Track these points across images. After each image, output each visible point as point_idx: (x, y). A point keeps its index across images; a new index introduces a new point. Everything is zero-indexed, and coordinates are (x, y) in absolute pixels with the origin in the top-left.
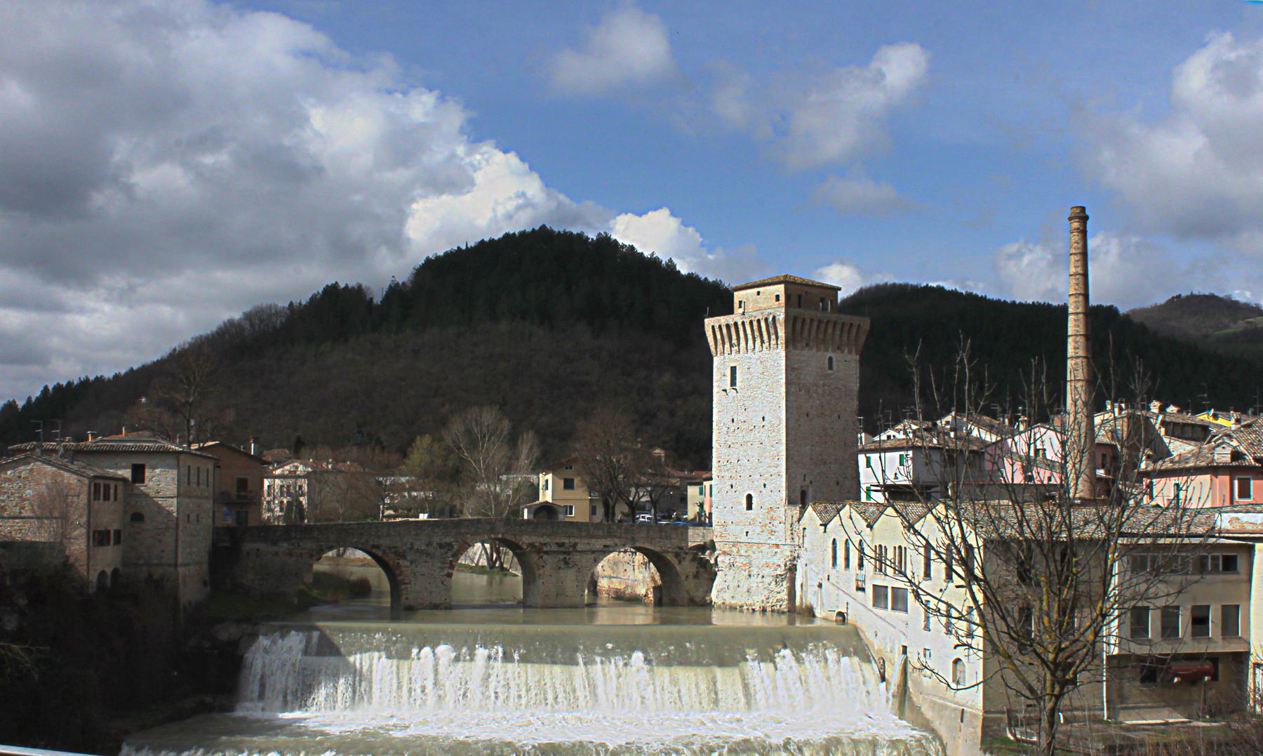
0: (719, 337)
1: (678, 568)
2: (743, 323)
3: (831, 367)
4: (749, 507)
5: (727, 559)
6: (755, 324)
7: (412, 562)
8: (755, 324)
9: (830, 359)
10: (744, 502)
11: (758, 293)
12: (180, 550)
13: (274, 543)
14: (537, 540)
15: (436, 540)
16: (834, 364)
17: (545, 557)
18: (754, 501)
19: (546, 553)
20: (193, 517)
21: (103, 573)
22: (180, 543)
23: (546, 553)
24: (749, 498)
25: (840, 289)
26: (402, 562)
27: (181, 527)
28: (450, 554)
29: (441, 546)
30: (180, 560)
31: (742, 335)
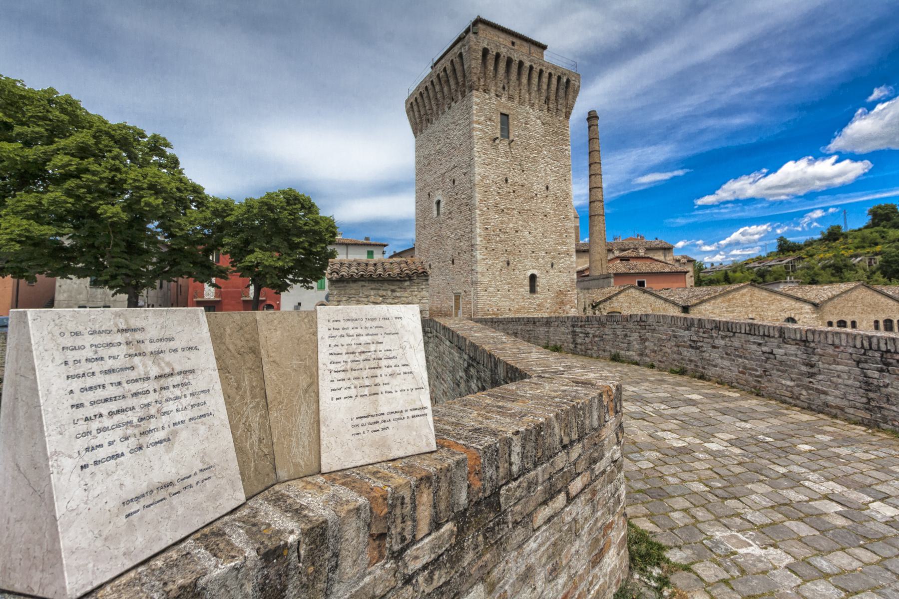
2: (531, 68)
4: (533, 290)
6: (546, 75)
8: (546, 75)
10: (527, 282)
18: (541, 282)
24: (533, 278)
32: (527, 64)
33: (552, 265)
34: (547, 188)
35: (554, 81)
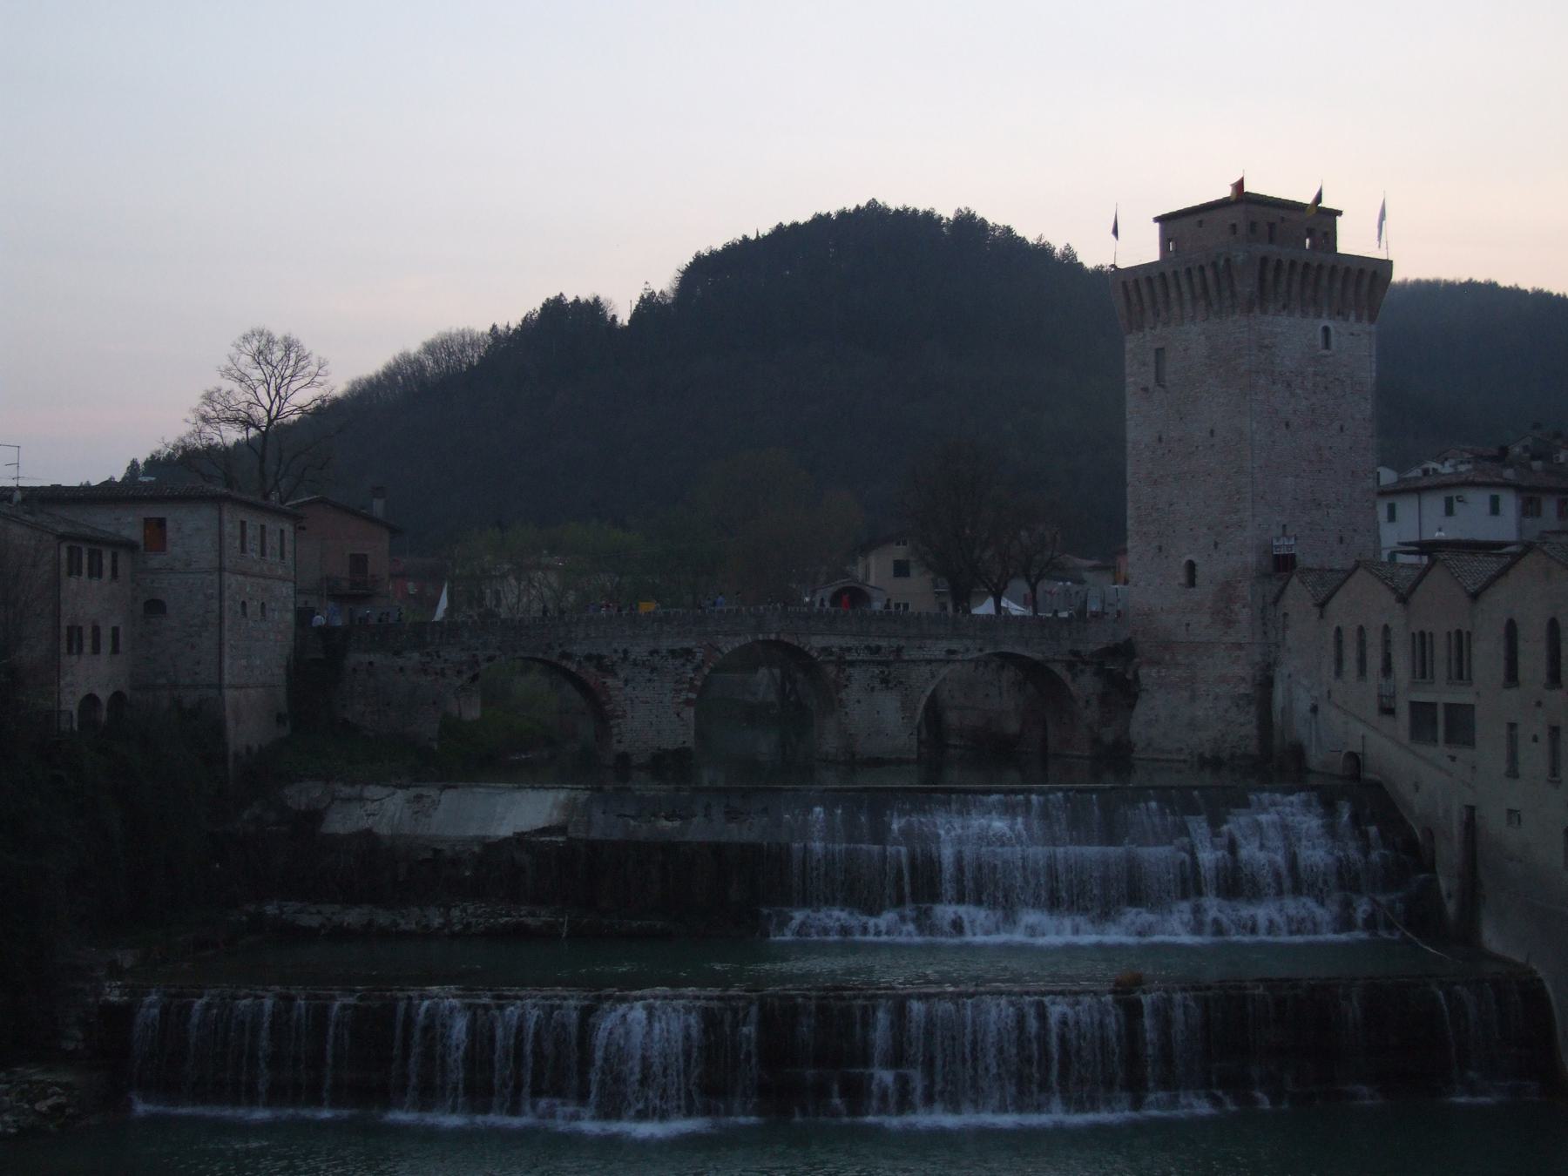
0: (1134, 298)
1: (1073, 688)
3: (1327, 345)
4: (1191, 582)
5: (1154, 672)
6: (1196, 273)
7: (626, 682)
8: (1196, 273)
9: (1326, 330)
11: (1200, 223)
12: (227, 662)
13: (397, 653)
14: (835, 642)
15: (665, 644)
16: (1333, 339)
17: (849, 670)
18: (1199, 570)
19: (852, 664)
20: (254, 606)
21: (91, 700)
22: (227, 649)
23: (852, 664)
24: (1191, 566)
25: (1339, 213)
26: (610, 681)
27: (227, 623)
28: (689, 667)
29: (673, 653)
30: (227, 678)
31: (1173, 295)
32: (1169, 274)
33: (1216, 545)
34: (1212, 432)
35: (1209, 274)
